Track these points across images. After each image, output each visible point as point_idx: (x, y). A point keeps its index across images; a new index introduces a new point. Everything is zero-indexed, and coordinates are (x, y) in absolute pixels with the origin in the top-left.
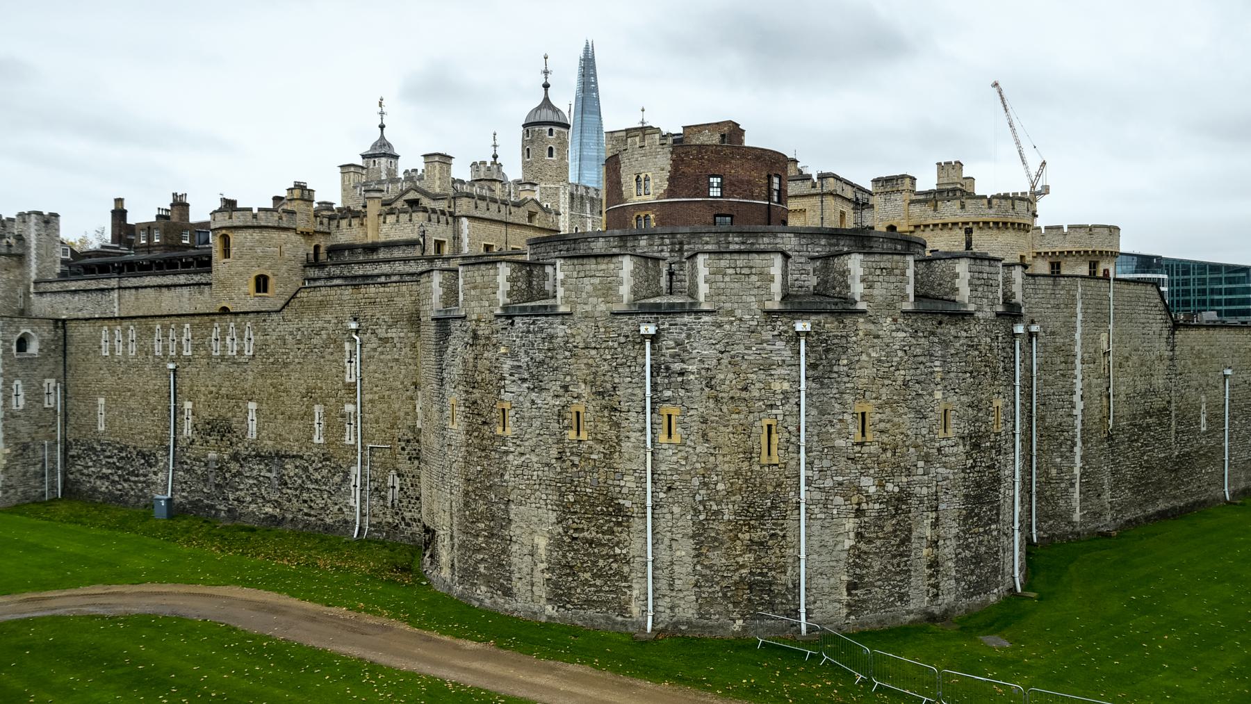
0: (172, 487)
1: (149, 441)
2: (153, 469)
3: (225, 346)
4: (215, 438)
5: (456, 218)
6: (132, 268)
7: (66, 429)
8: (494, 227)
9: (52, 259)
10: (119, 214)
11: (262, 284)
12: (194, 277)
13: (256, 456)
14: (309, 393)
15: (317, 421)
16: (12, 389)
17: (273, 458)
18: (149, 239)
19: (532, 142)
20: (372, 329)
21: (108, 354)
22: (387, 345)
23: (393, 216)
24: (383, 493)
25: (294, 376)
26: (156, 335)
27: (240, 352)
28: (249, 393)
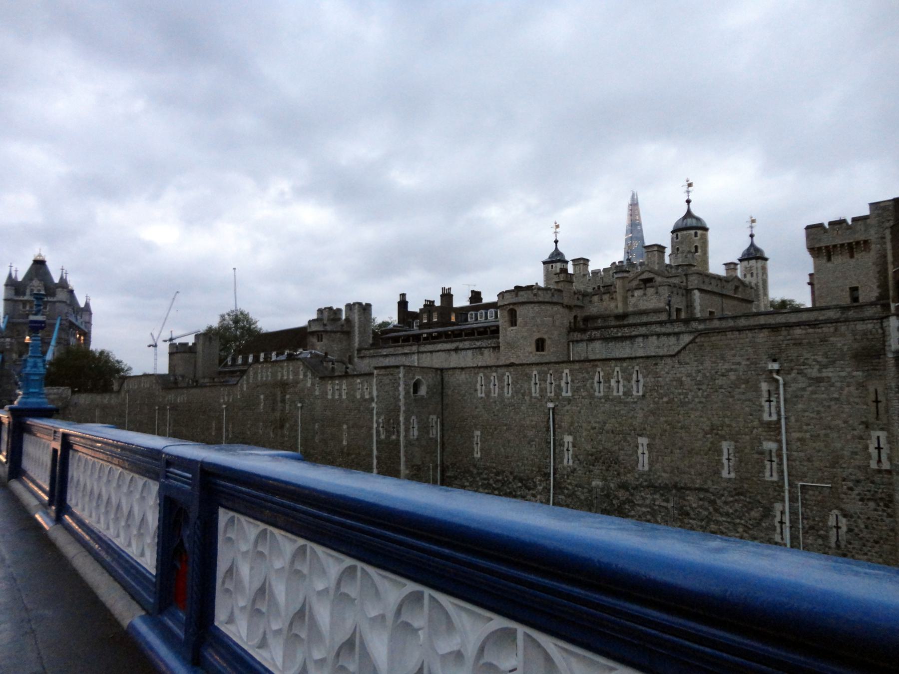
1: (526, 468)
2: (531, 492)
3: (609, 387)
4: (600, 468)
5: (688, 292)
6: (417, 338)
10: (403, 304)
11: (540, 345)
13: (648, 487)
14: (713, 428)
15: (725, 456)
16: (410, 423)
18: (430, 318)
19: (682, 243)
20: (798, 369)
21: (483, 395)
22: (822, 384)
23: (640, 290)
24: (822, 532)
26: (533, 379)
27: (627, 393)
28: (638, 429)
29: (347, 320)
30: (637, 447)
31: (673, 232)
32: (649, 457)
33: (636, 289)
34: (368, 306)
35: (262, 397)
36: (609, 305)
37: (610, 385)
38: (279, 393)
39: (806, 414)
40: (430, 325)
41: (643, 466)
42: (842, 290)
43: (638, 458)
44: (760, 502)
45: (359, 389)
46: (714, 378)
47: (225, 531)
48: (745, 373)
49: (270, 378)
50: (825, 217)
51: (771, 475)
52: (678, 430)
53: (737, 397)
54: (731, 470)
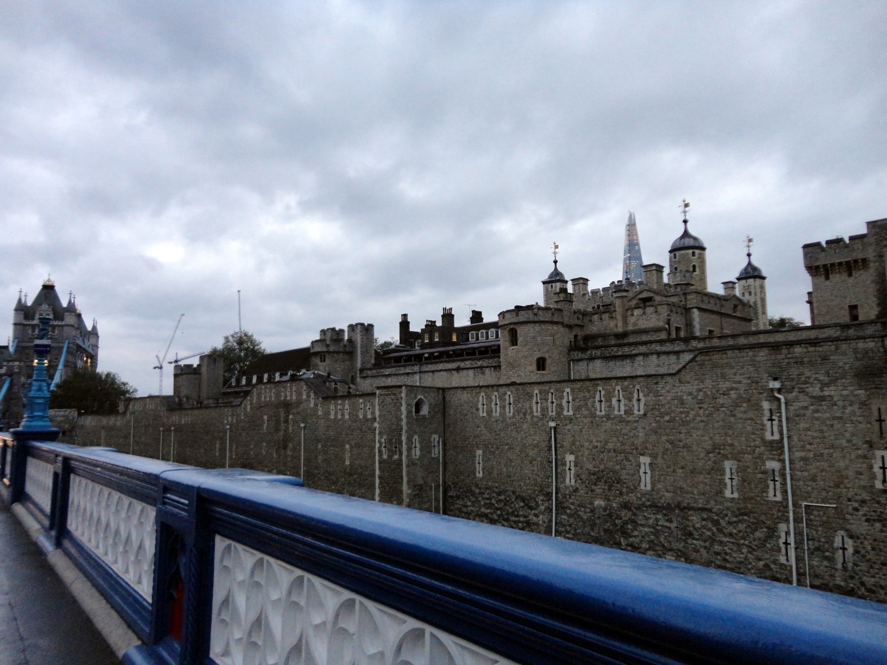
0: (555, 529)
2: (533, 512)
3: (610, 406)
4: (602, 487)
5: (687, 310)
6: (419, 359)
7: (445, 475)
8: (714, 316)
9: (369, 355)
10: (404, 324)
11: (541, 364)
12: (477, 362)
13: (651, 506)
14: (715, 447)
15: (728, 475)
17: (674, 511)
18: (431, 338)
19: (679, 262)
20: (800, 388)
22: (824, 403)
23: (640, 310)
24: (827, 554)
25: (695, 434)
26: (535, 398)
27: (629, 412)
29: (350, 340)
30: (640, 467)
31: (670, 252)
32: (652, 477)
33: (635, 308)
34: (371, 326)
35: (265, 417)
36: (609, 324)
37: (611, 404)
38: (283, 412)
39: (809, 433)
40: (432, 345)
41: (646, 486)
42: (842, 308)
43: (640, 477)
44: (764, 523)
45: (361, 409)
46: (715, 396)
47: (222, 560)
48: (746, 392)
49: (273, 399)
50: (822, 237)
51: (775, 495)
52: (681, 450)
53: (738, 415)
54: (734, 489)
